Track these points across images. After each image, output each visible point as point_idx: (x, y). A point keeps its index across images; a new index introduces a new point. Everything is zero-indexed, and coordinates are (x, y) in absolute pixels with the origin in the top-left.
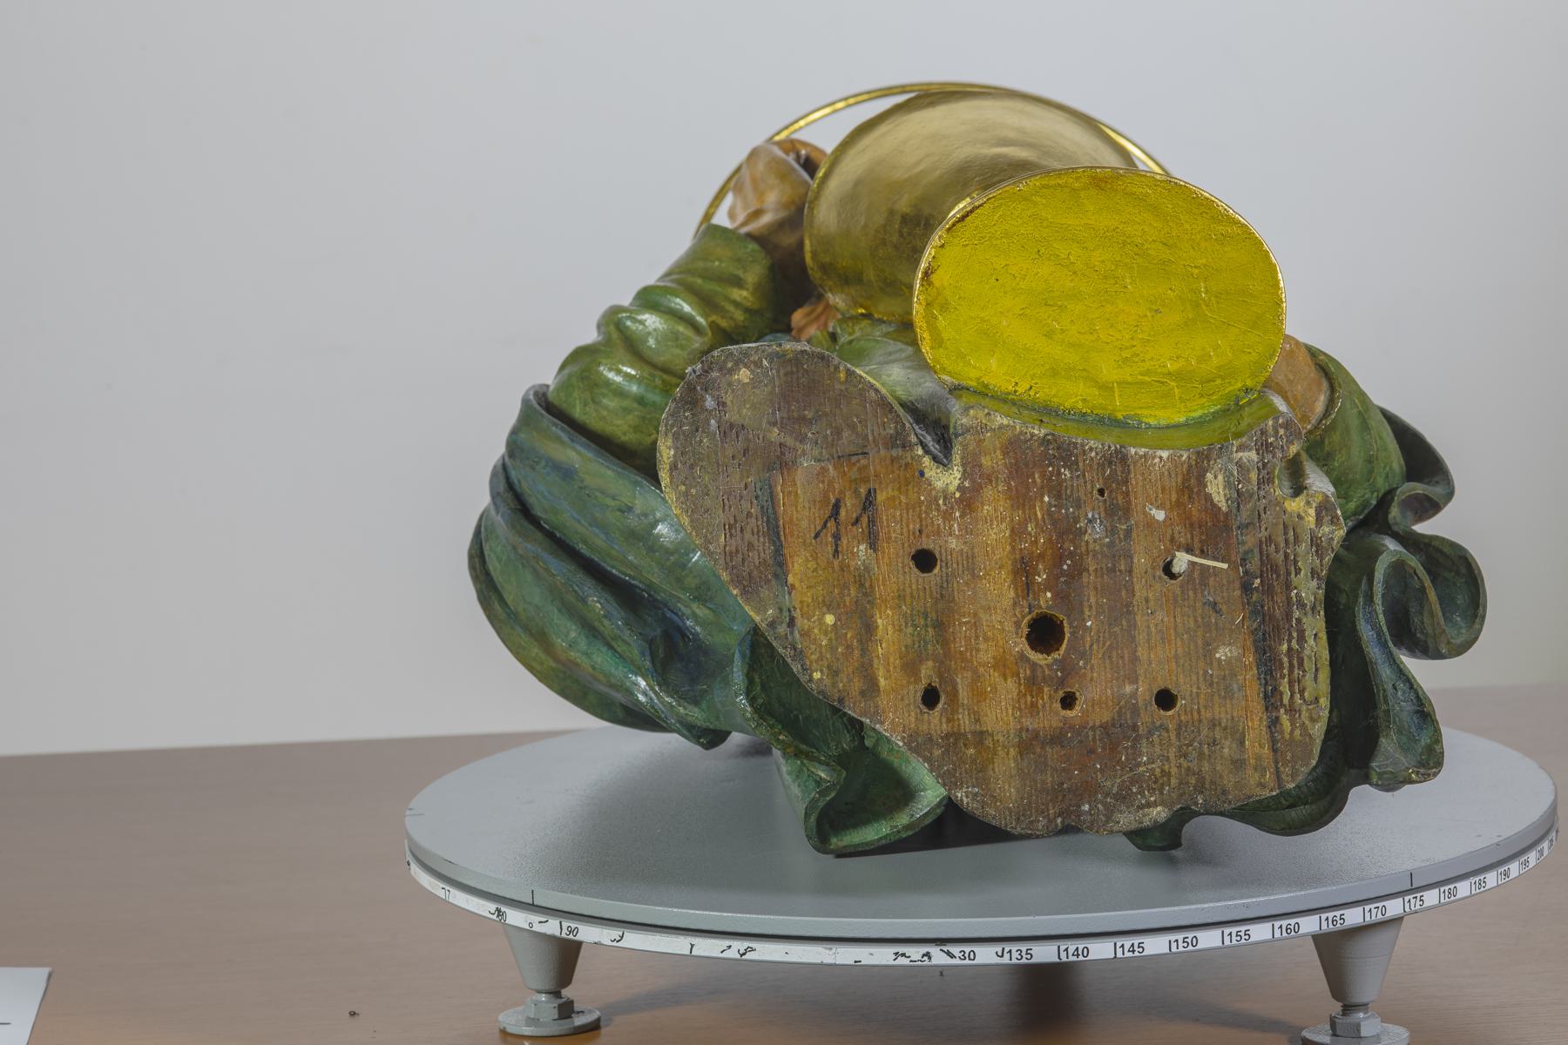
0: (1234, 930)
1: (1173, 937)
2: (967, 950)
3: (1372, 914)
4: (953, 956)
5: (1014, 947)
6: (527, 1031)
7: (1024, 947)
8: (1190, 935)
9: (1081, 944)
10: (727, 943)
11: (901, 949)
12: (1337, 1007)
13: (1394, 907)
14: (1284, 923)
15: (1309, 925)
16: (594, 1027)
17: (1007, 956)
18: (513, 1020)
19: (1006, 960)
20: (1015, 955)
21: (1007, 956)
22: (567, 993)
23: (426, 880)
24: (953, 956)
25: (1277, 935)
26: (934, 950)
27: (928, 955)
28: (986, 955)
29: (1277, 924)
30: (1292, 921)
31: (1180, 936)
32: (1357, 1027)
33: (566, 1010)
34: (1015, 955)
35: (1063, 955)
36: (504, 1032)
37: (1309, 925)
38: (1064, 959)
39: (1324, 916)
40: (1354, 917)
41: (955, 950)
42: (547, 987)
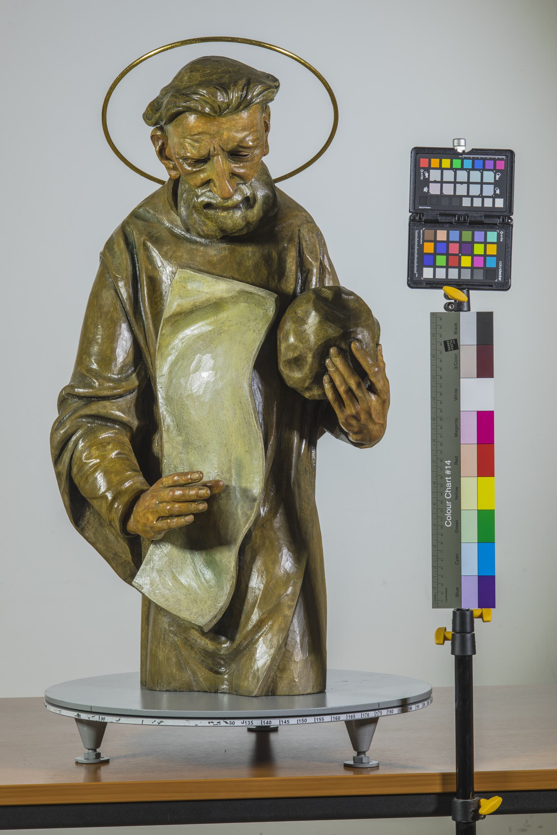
0: (319, 717)
1: (299, 719)
2: (232, 721)
3: (364, 716)
4: (227, 723)
5: (247, 721)
8: (304, 718)
11: (211, 721)
12: (355, 754)
13: (372, 714)
14: (335, 716)
17: (245, 723)
19: (244, 724)
20: (247, 723)
21: (245, 723)
24: (227, 723)
25: (333, 720)
26: (222, 721)
27: (219, 722)
28: (238, 722)
29: (333, 716)
30: (338, 716)
31: (301, 719)
32: (362, 759)
34: (247, 723)
35: (263, 723)
37: (343, 717)
38: (263, 725)
39: (348, 715)
40: (358, 716)
41: (228, 721)
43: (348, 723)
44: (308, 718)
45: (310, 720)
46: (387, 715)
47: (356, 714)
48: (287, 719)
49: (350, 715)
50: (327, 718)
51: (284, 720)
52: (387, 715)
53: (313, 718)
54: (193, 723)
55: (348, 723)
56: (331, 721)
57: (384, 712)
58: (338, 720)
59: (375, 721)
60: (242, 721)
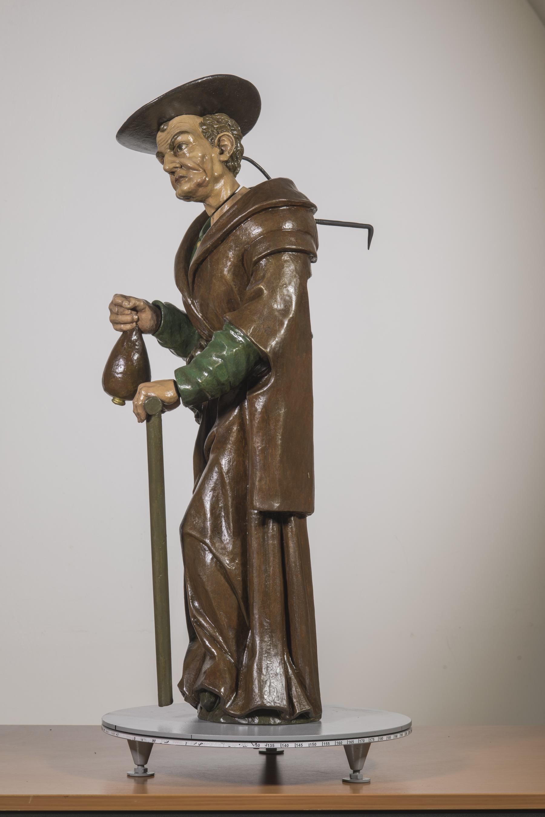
0: (325, 742)
1: (310, 743)
5: (270, 744)
6: (137, 775)
7: (272, 744)
8: (314, 742)
9: (287, 744)
10: (195, 742)
13: (367, 740)
15: (345, 742)
16: (152, 776)
18: (132, 772)
19: (267, 747)
22: (146, 766)
23: (110, 732)
33: (146, 770)
36: (129, 776)
40: (356, 741)
42: (142, 764)
43: (346, 747)
44: (317, 742)
45: (319, 744)
46: (378, 741)
47: (355, 740)
48: (301, 743)
49: (350, 740)
50: (332, 743)
51: (298, 743)
52: (378, 741)
53: (321, 742)
54: (226, 745)
55: (346, 747)
56: (335, 745)
57: (376, 739)
58: (340, 744)
59: (367, 746)
60: (266, 744)
